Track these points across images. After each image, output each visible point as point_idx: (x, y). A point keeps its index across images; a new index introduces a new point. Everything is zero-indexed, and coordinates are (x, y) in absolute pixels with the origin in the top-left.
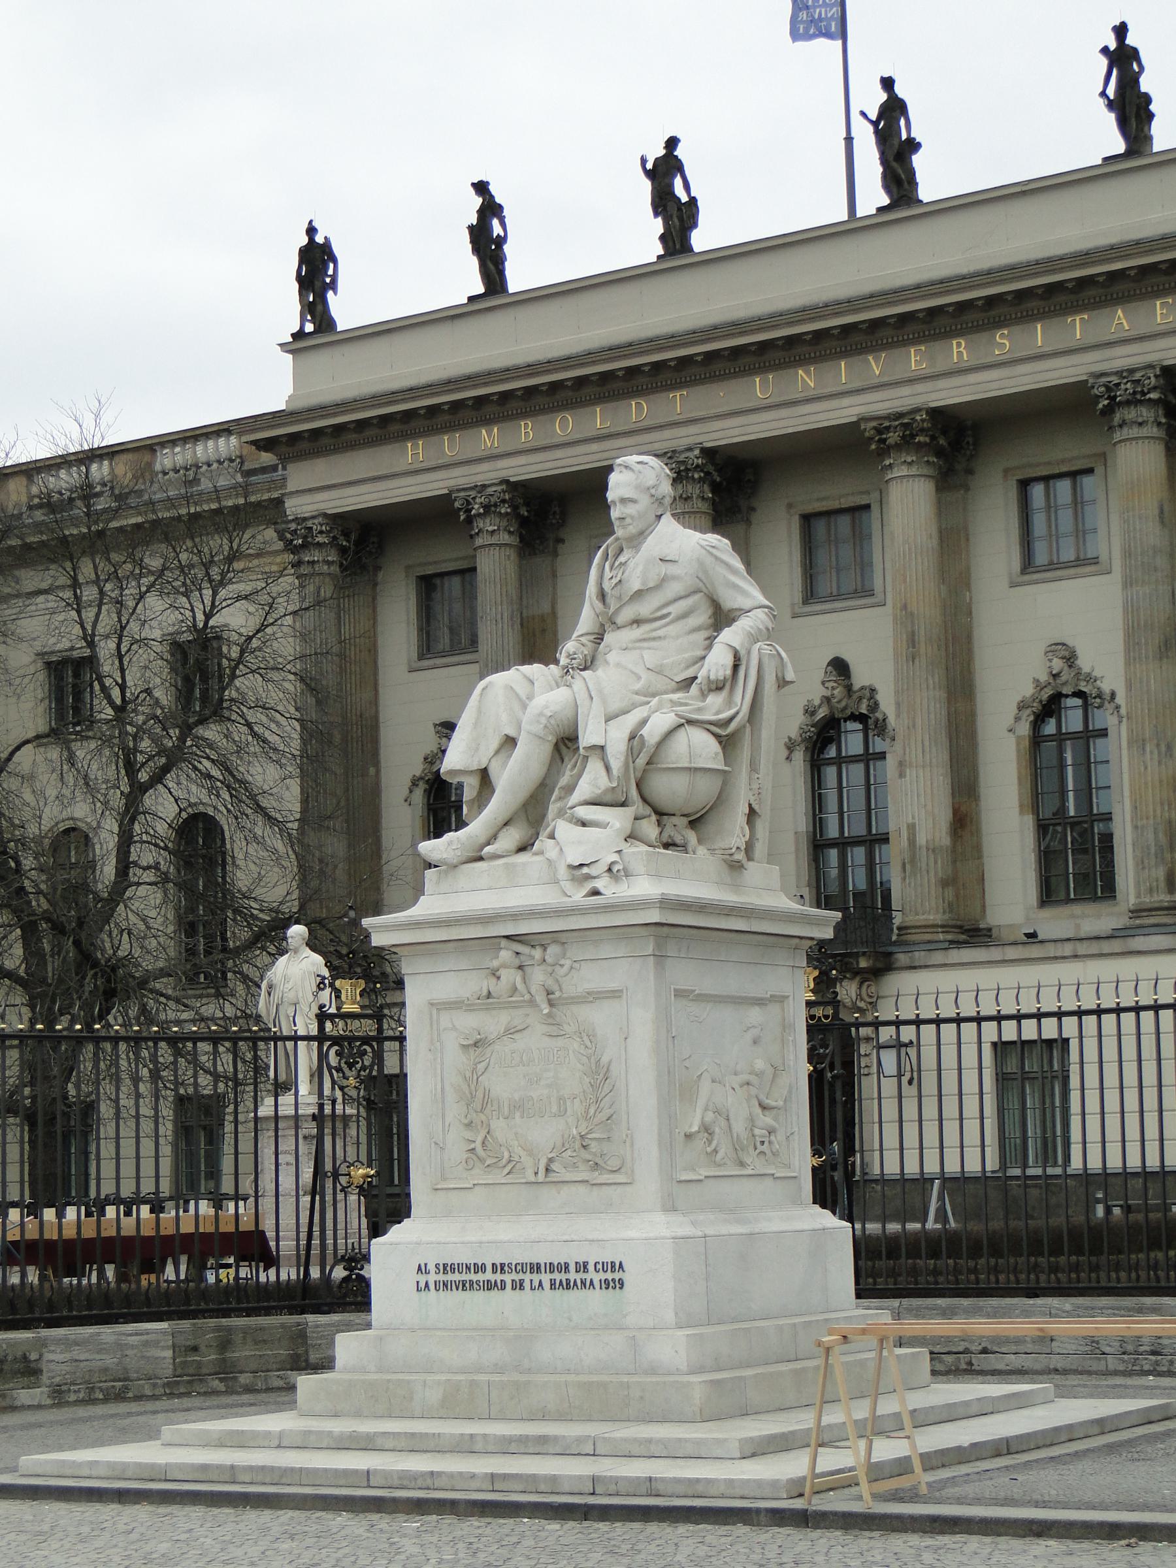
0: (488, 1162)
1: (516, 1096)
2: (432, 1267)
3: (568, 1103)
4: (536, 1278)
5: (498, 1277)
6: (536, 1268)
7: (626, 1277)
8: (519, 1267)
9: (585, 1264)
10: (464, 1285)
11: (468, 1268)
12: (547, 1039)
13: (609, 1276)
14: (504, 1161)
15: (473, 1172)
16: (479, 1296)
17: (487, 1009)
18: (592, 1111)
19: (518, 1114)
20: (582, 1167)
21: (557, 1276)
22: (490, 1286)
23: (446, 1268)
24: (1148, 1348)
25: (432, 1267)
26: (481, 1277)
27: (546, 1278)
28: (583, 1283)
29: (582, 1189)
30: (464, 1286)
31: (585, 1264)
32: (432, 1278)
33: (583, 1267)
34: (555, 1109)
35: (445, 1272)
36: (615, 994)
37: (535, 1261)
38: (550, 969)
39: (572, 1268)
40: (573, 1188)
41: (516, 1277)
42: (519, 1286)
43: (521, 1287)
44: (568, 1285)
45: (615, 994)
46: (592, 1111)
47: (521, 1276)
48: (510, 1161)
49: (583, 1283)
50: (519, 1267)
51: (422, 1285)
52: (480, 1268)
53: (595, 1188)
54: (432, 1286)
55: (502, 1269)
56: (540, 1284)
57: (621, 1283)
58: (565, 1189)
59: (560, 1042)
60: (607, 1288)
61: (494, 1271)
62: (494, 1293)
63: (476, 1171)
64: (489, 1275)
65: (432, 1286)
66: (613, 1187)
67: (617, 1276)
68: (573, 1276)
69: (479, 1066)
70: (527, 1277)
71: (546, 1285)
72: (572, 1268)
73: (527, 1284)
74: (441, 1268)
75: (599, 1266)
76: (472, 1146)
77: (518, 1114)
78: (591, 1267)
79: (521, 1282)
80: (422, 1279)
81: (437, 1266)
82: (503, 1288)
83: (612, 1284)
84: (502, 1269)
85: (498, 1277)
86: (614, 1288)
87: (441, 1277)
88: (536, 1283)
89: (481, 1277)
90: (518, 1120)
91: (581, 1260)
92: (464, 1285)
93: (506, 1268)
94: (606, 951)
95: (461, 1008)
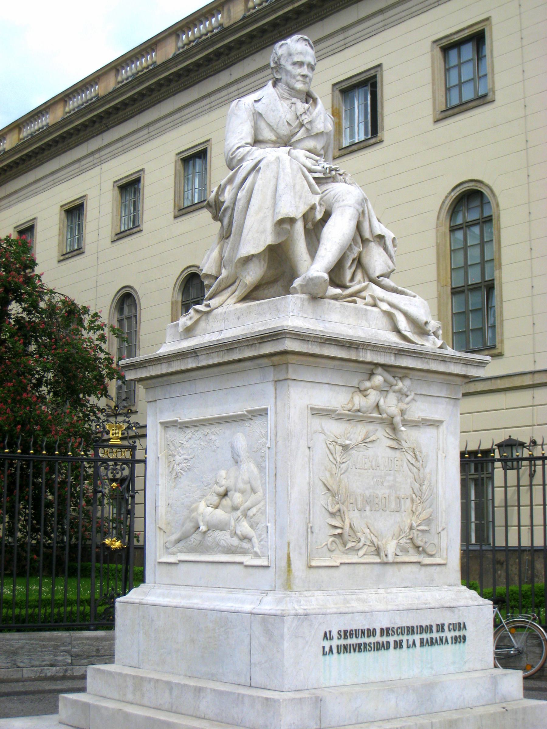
0: (350, 545)
1: (367, 493)
2: (335, 634)
3: (402, 500)
4: (411, 638)
5: (385, 639)
6: (410, 630)
7: (466, 633)
8: (399, 631)
9: (443, 625)
10: (360, 648)
11: (363, 632)
12: (388, 450)
13: (457, 633)
14: (361, 544)
15: (334, 553)
16: (369, 656)
17: (349, 420)
18: (420, 509)
19: (368, 508)
20: (412, 551)
21: (425, 636)
22: (379, 647)
23: (346, 634)
24: (48, 663)
25: (335, 634)
26: (372, 640)
27: (417, 638)
28: (441, 640)
29: (415, 568)
30: (360, 648)
31: (443, 625)
32: (335, 643)
33: (441, 628)
34: (393, 506)
35: (345, 637)
36: (436, 424)
37: (410, 625)
38: (400, 396)
39: (434, 629)
40: (409, 568)
41: (397, 638)
42: (398, 645)
43: (401, 647)
44: (432, 642)
45: (436, 424)
46: (420, 509)
47: (400, 637)
48: (365, 545)
49: (441, 640)
50: (399, 631)
51: (327, 649)
52: (371, 633)
53: (423, 569)
54: (335, 650)
55: (388, 633)
56: (414, 643)
57: (464, 638)
58: (405, 568)
59: (397, 454)
60: (455, 643)
61: (382, 635)
62: (382, 652)
63: (337, 552)
64: (378, 638)
65: (335, 650)
66: (434, 567)
67: (461, 633)
68: (435, 635)
69: (342, 466)
70: (404, 638)
71: (418, 643)
72: (434, 629)
73: (404, 644)
74: (342, 634)
75: (451, 627)
76: (339, 531)
77: (368, 508)
78: (446, 628)
79: (401, 641)
80: (327, 644)
81: (339, 633)
82: (388, 648)
83: (459, 640)
84: (388, 633)
85: (385, 639)
86: (460, 643)
87: (342, 642)
88: (411, 642)
89: (372, 640)
90: (368, 512)
91: (439, 623)
92: (360, 648)
93: (390, 632)
94: (435, 390)
95: (329, 416)
